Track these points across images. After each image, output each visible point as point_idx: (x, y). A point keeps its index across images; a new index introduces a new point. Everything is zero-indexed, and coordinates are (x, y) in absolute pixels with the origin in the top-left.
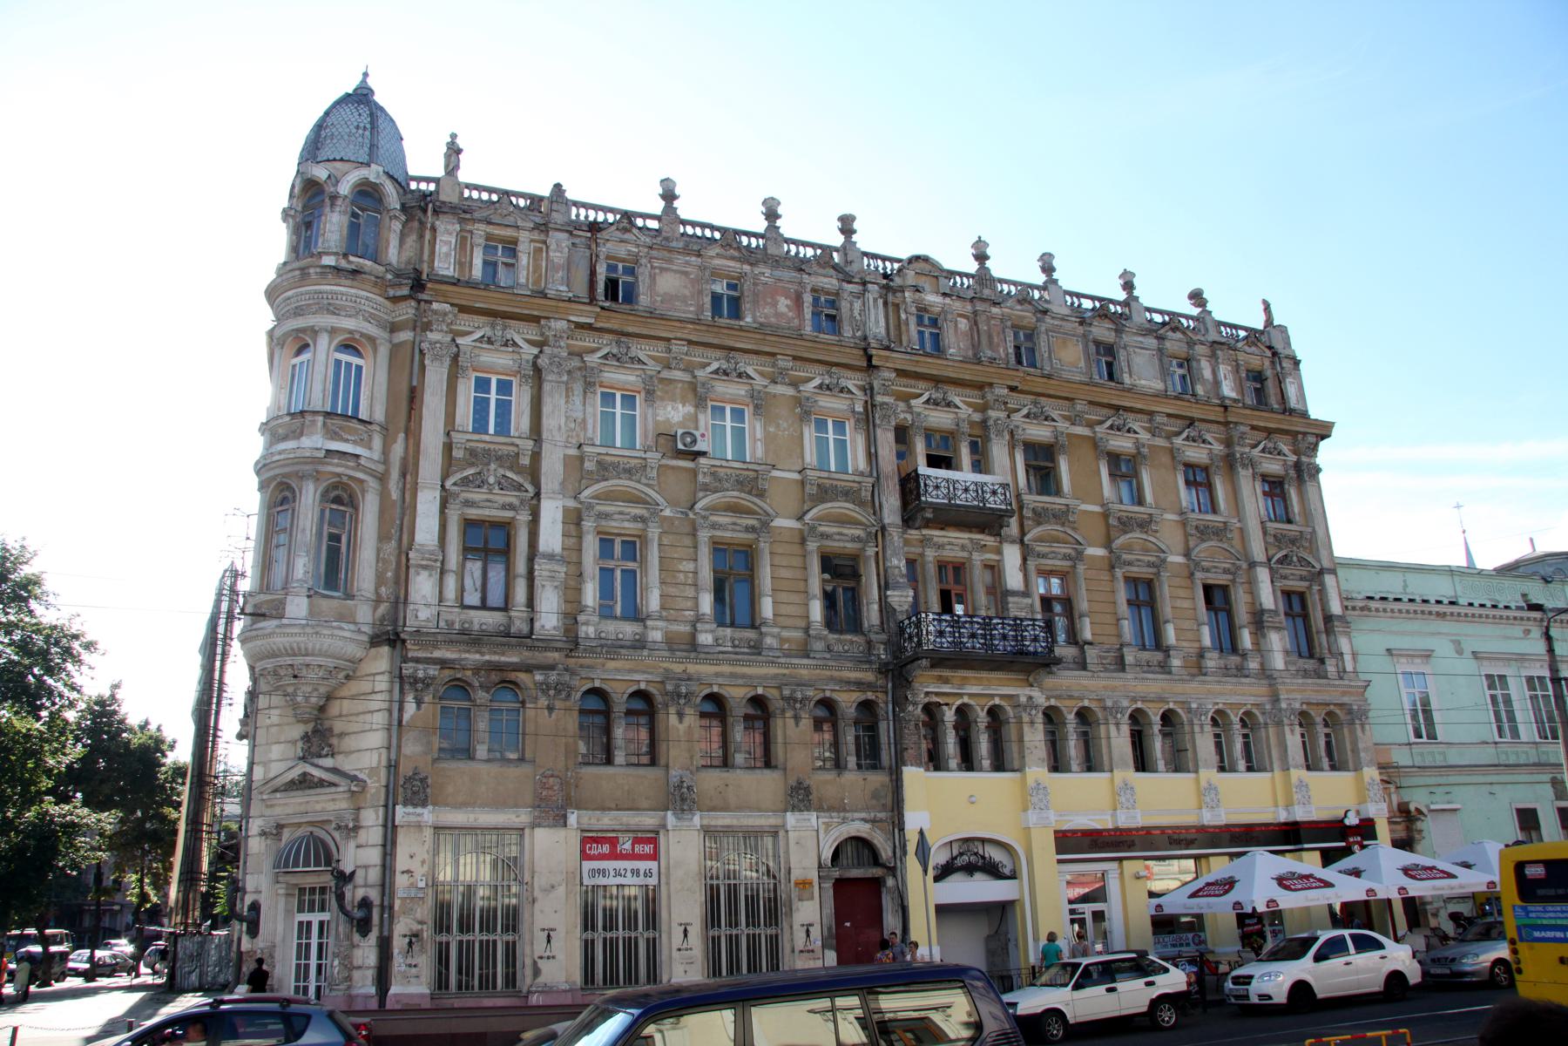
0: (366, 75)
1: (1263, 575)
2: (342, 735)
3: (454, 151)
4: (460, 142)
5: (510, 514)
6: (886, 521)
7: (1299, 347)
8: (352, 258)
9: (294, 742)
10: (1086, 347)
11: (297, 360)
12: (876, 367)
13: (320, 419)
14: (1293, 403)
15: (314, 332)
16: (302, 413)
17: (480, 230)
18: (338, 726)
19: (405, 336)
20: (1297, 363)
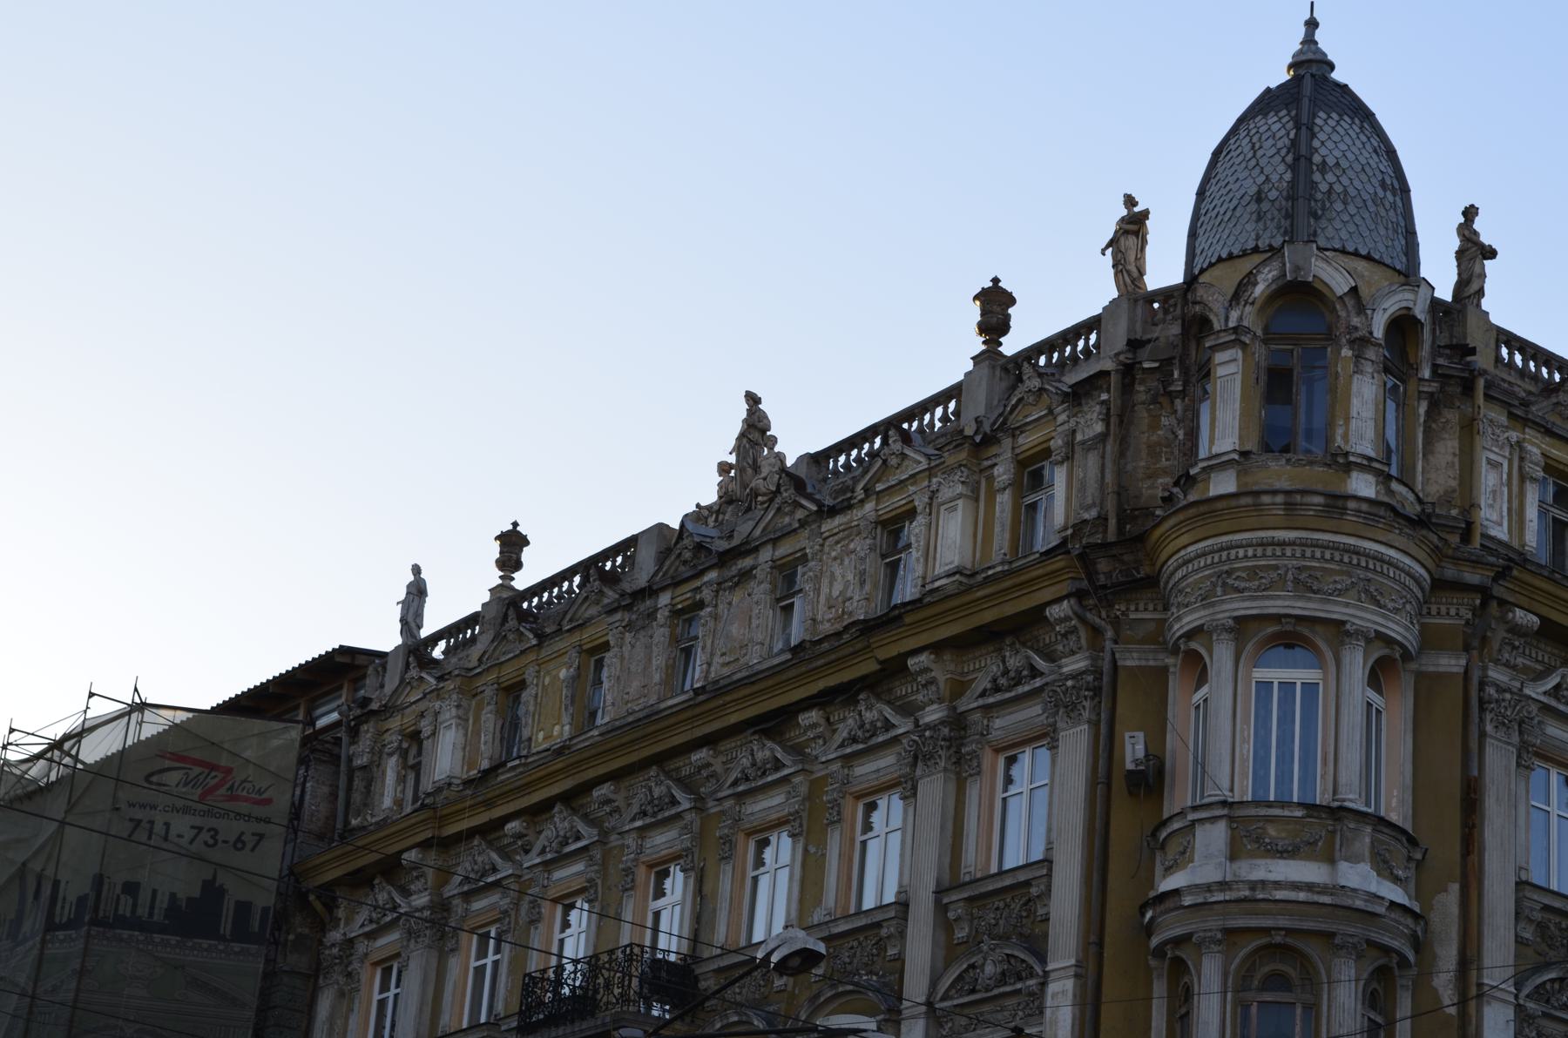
0: (1312, 24)
3: (1473, 253)
4: (1486, 230)
8: (1395, 486)
11: (1275, 675)
13: (1369, 829)
15: (1339, 631)
16: (1338, 813)
17: (1536, 446)
19: (1450, 663)
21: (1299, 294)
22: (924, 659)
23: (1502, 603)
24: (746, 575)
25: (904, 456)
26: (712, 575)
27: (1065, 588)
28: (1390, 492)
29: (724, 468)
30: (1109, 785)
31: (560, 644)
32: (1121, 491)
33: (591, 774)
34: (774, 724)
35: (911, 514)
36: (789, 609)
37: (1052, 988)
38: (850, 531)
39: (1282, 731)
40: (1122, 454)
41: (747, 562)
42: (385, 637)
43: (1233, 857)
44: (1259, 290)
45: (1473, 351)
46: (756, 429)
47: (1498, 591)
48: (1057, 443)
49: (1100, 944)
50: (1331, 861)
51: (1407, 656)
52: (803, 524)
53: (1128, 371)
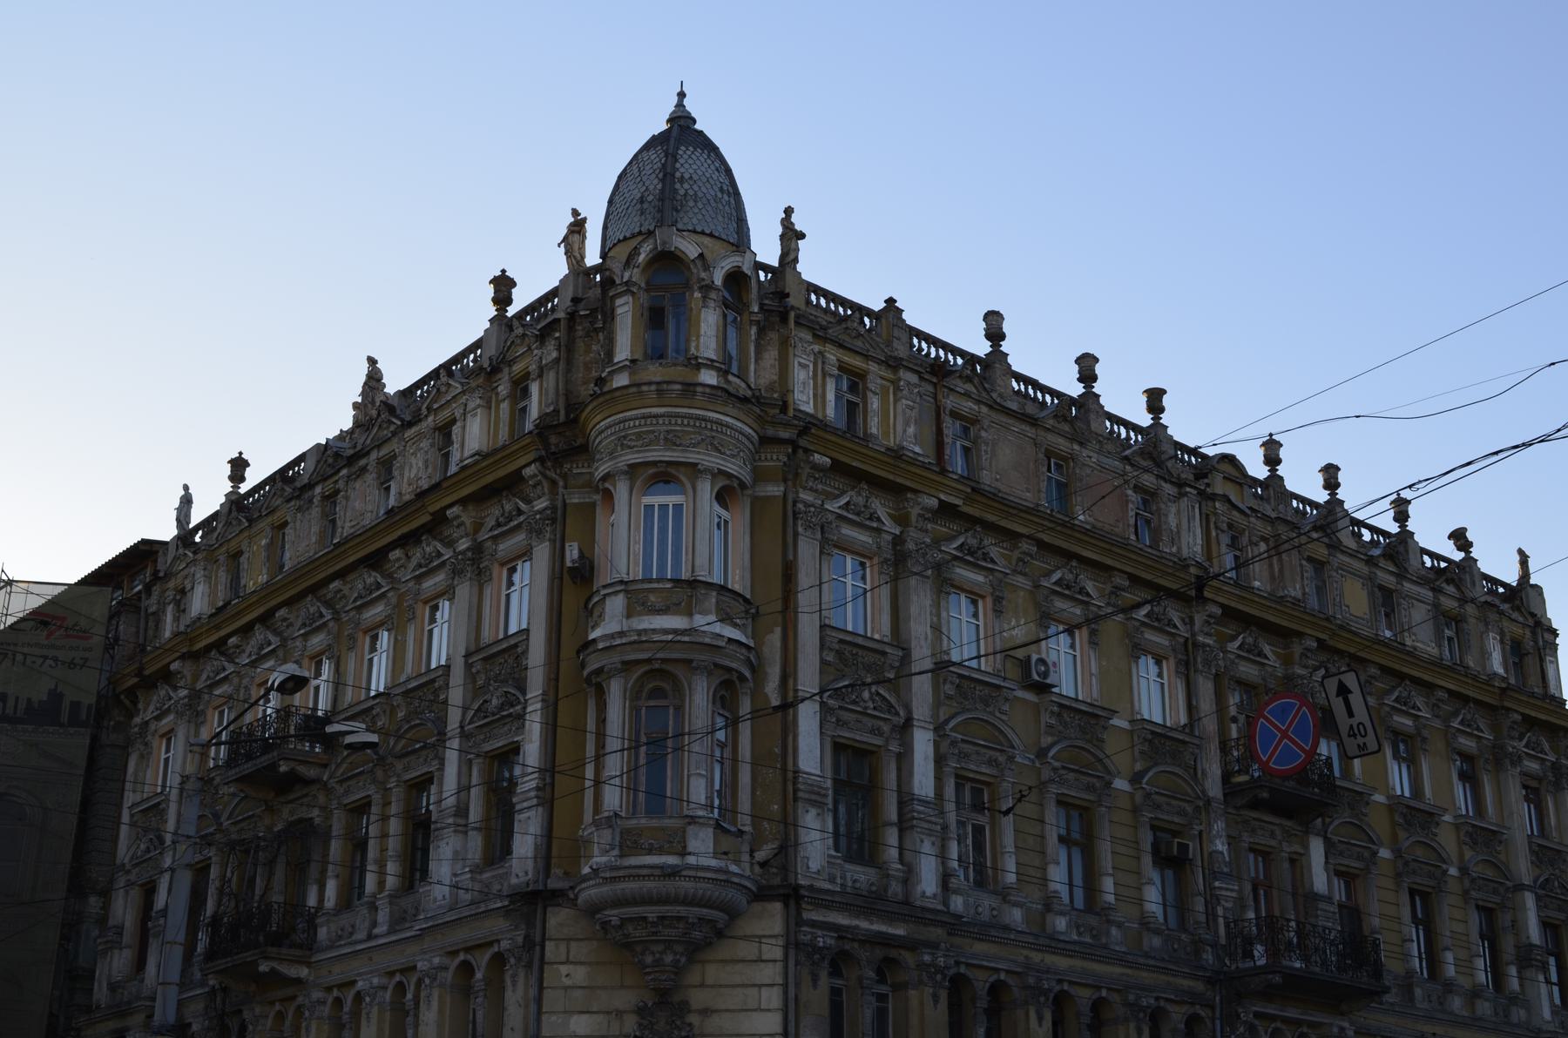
0: (682, 95)
1: (1530, 900)
2: (706, 1012)
3: (791, 236)
4: (799, 223)
5: (878, 741)
6: (1211, 794)
7: (1555, 613)
8: (731, 378)
9: (619, 1014)
10: (1371, 594)
11: (656, 500)
12: (1206, 600)
14: (1553, 691)
15: (694, 469)
16: (693, 584)
17: (832, 355)
18: (698, 998)
19: (775, 490)
20: (1555, 633)
21: (667, 259)
22: (455, 510)
23: (806, 451)
24: (364, 470)
25: (449, 385)
26: (344, 472)
27: (531, 457)
28: (728, 382)
29: (356, 406)
30: (561, 578)
31: (262, 524)
32: (568, 394)
34: (375, 560)
35: (454, 421)
36: (388, 489)
38: (420, 436)
39: (670, 536)
40: (568, 371)
41: (363, 462)
42: (166, 531)
43: (629, 616)
45: (788, 295)
46: (374, 379)
47: (802, 442)
48: (533, 367)
49: (557, 680)
50: (690, 615)
51: (743, 485)
52: (394, 434)
53: (572, 316)
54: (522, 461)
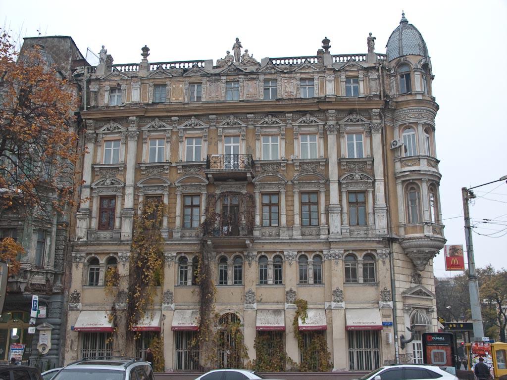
0: (403, 14)
27: (380, 107)
29: (228, 53)
33: (211, 112)
37: (377, 183)
44: (422, 63)
52: (275, 73)
54: (375, 107)
